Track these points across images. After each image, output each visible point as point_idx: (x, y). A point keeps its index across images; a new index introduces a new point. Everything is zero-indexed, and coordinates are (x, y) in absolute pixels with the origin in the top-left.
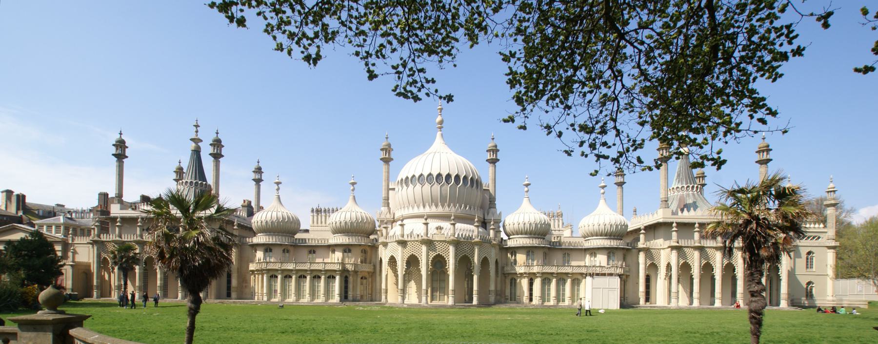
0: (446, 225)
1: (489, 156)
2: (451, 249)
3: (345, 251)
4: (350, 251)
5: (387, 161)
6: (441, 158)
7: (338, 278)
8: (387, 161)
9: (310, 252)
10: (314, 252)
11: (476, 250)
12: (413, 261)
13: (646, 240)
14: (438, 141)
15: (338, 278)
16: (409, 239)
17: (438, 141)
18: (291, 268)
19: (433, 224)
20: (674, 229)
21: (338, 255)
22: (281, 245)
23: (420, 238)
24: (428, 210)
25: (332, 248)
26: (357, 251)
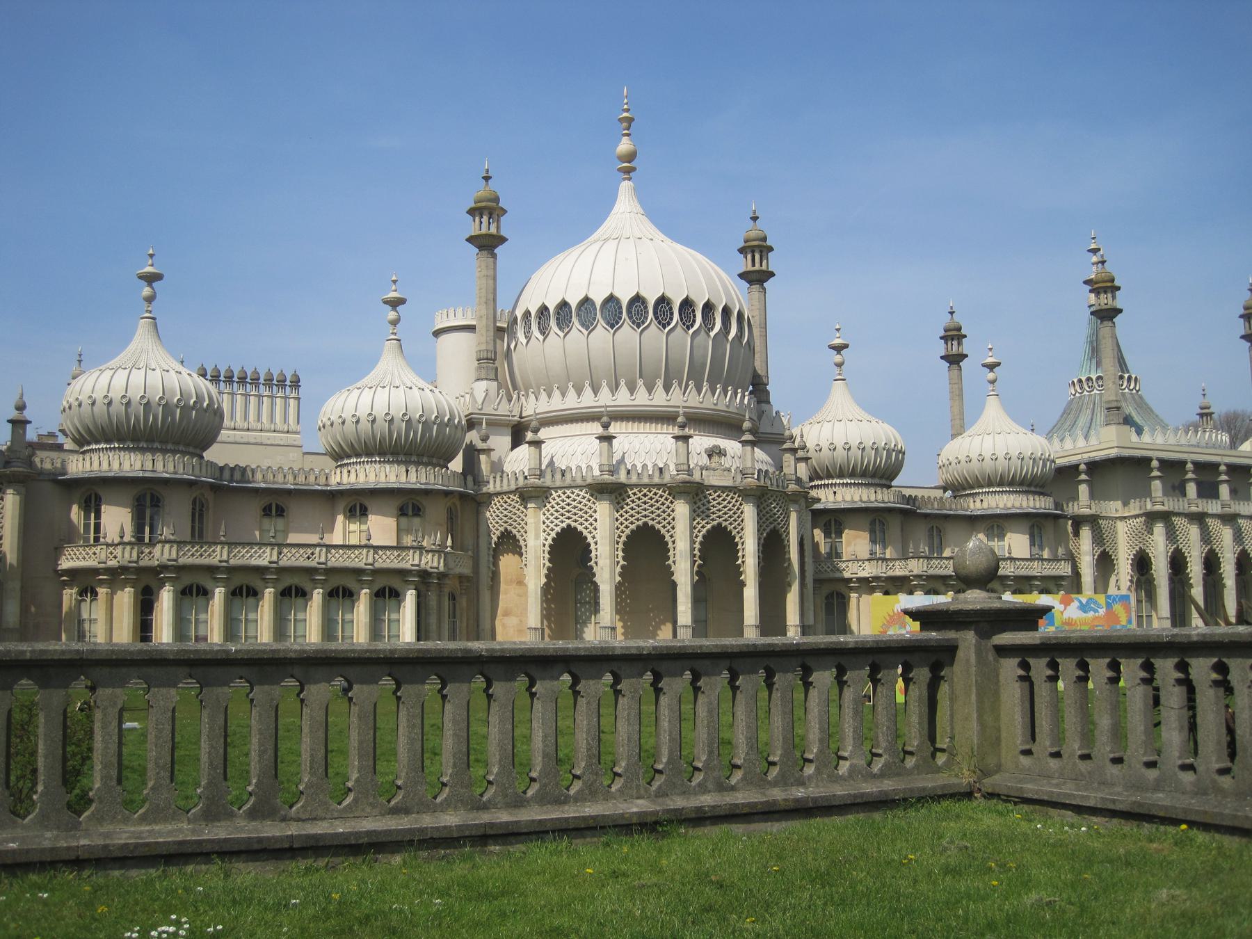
0: (732, 446)
1: (744, 264)
2: (749, 512)
3: (402, 512)
4: (417, 511)
5: (487, 244)
6: (629, 252)
7: (410, 597)
8: (487, 244)
9: (267, 512)
10: (281, 512)
11: (793, 517)
12: (645, 547)
13: (1092, 496)
14: (626, 204)
15: (410, 597)
16: (634, 479)
17: (626, 204)
18: (263, 562)
19: (701, 442)
20: (1156, 473)
21: (382, 527)
22: (191, 484)
23: (667, 479)
24: (681, 399)
25: (358, 503)
26: (435, 512)
